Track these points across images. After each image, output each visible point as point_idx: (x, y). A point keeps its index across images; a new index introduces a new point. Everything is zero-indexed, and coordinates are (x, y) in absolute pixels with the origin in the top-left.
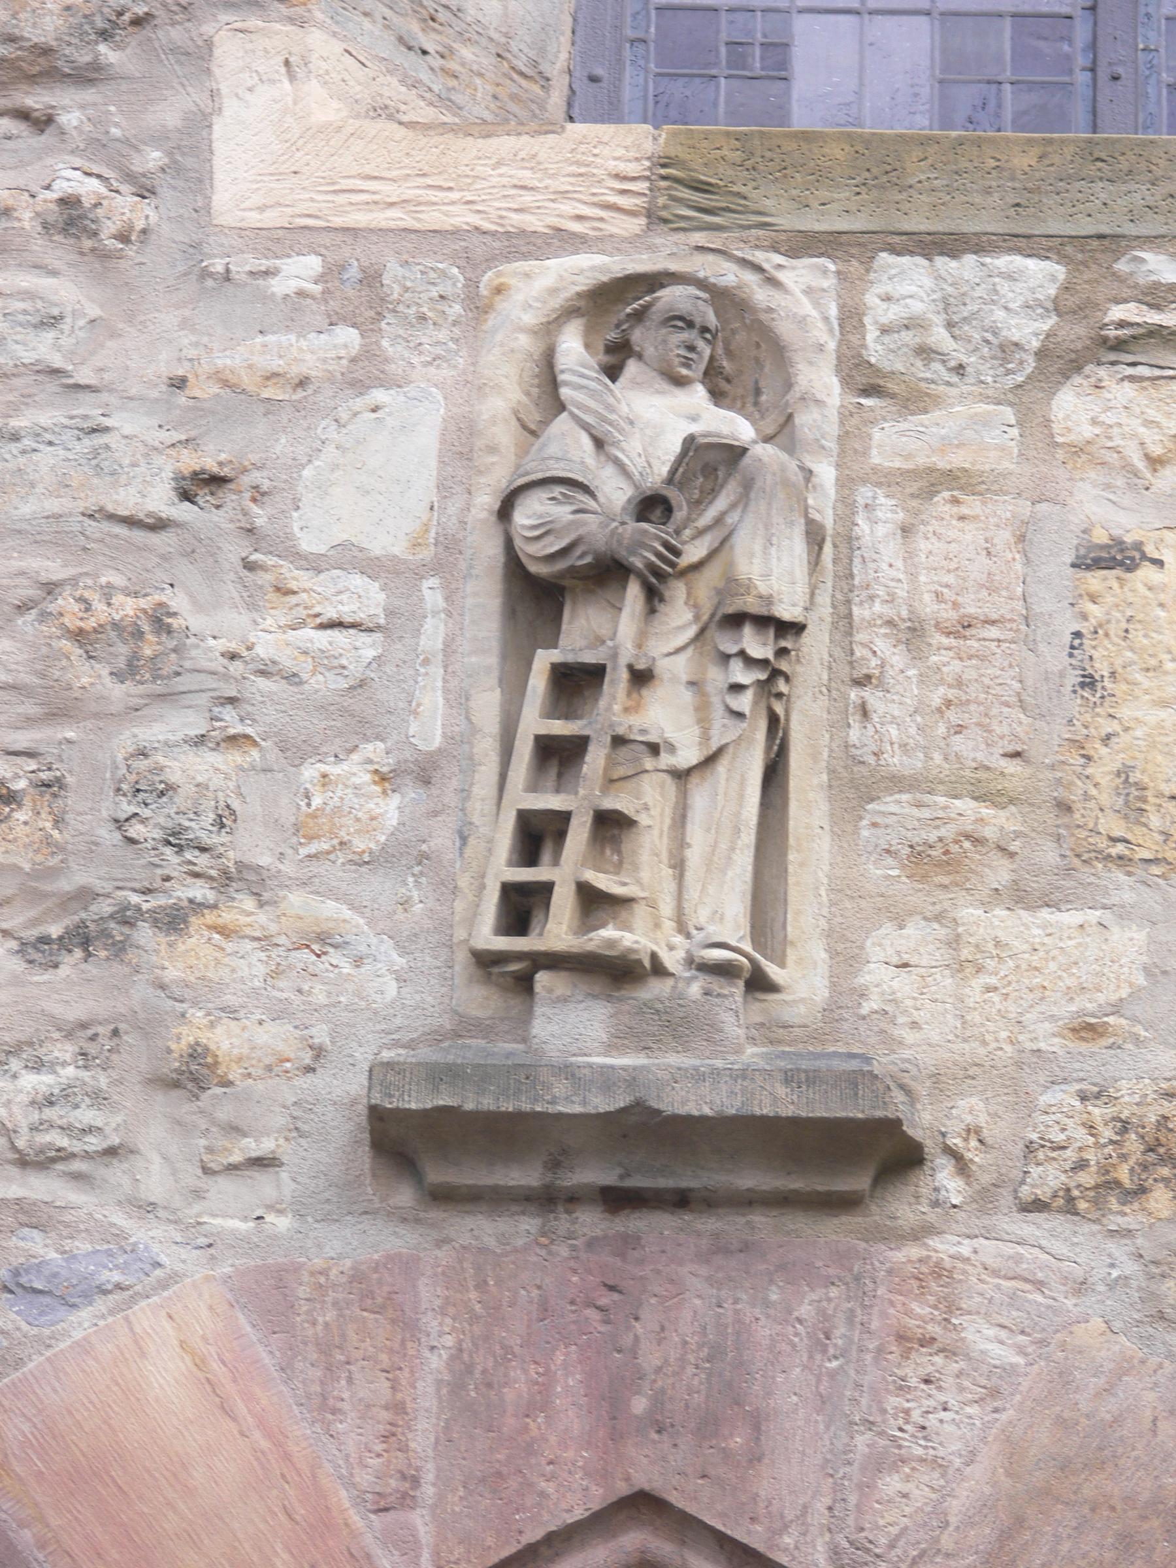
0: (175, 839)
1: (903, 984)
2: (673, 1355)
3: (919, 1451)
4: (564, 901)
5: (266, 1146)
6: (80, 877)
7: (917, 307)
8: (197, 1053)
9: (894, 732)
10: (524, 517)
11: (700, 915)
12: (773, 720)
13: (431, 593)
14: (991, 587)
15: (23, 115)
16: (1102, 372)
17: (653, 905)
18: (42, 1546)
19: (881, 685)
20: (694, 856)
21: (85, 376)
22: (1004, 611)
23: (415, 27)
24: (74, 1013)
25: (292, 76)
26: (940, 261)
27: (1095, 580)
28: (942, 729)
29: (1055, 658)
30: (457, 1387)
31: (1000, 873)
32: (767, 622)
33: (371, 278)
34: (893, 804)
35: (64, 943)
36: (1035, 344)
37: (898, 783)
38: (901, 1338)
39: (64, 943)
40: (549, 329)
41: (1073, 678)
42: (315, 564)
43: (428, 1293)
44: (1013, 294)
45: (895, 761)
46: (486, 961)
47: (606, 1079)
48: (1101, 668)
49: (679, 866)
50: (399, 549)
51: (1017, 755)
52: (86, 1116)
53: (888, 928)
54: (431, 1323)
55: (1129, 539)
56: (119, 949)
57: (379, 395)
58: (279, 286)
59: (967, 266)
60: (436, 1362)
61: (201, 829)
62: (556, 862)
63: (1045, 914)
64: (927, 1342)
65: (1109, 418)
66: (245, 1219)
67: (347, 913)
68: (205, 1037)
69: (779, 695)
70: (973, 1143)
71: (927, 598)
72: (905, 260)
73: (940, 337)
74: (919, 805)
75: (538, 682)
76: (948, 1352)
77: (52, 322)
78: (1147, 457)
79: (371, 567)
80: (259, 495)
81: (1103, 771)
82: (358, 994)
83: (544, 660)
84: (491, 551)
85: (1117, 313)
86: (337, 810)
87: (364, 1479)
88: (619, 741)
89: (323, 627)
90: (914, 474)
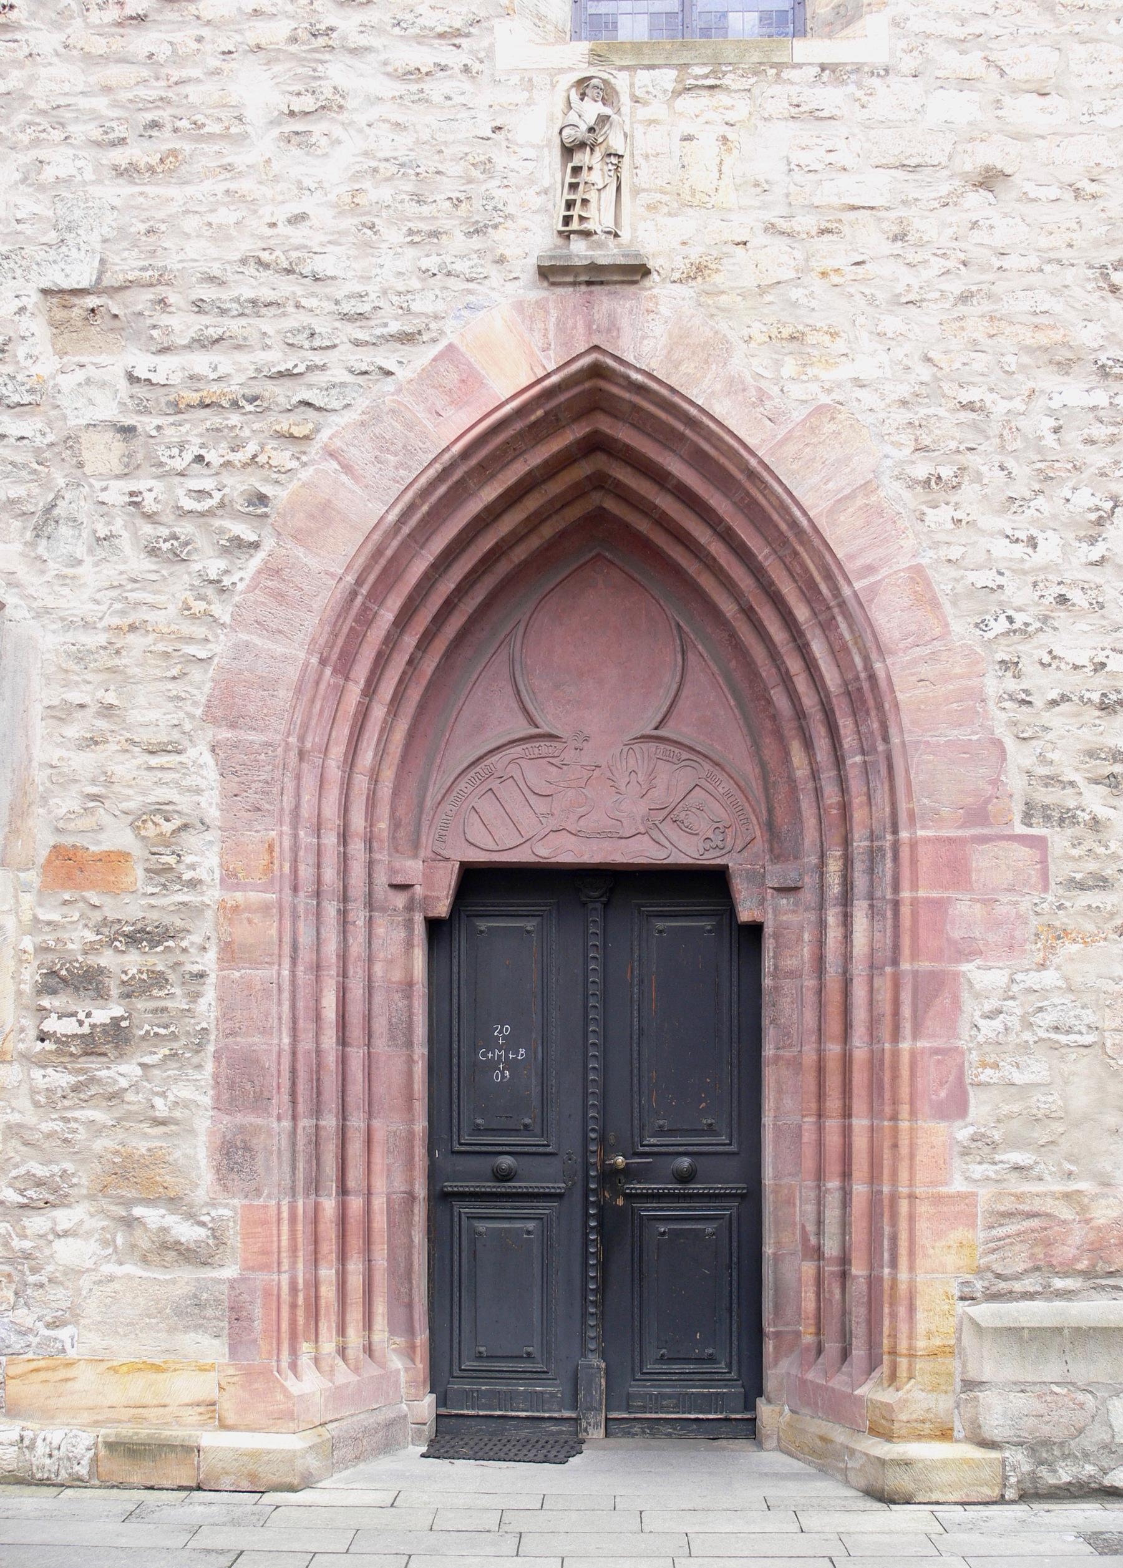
0: (495, 209)
4: (576, 219)
6: (476, 218)
8: (501, 255)
10: (565, 133)
13: (546, 150)
15: (454, 45)
21: (470, 106)
24: (476, 248)
27: (685, 143)
30: (558, 325)
31: (665, 209)
32: (615, 155)
33: (530, 80)
34: (643, 195)
37: (644, 190)
40: (569, 90)
43: (551, 305)
45: (643, 186)
46: (560, 233)
47: (586, 257)
49: (599, 210)
52: (480, 270)
54: (552, 311)
56: (485, 233)
60: (553, 319)
61: (500, 206)
73: (651, 89)
75: (569, 170)
77: (463, 93)
79: (533, 146)
80: (509, 131)
81: (687, 186)
83: (570, 165)
85: (688, 82)
87: (540, 344)
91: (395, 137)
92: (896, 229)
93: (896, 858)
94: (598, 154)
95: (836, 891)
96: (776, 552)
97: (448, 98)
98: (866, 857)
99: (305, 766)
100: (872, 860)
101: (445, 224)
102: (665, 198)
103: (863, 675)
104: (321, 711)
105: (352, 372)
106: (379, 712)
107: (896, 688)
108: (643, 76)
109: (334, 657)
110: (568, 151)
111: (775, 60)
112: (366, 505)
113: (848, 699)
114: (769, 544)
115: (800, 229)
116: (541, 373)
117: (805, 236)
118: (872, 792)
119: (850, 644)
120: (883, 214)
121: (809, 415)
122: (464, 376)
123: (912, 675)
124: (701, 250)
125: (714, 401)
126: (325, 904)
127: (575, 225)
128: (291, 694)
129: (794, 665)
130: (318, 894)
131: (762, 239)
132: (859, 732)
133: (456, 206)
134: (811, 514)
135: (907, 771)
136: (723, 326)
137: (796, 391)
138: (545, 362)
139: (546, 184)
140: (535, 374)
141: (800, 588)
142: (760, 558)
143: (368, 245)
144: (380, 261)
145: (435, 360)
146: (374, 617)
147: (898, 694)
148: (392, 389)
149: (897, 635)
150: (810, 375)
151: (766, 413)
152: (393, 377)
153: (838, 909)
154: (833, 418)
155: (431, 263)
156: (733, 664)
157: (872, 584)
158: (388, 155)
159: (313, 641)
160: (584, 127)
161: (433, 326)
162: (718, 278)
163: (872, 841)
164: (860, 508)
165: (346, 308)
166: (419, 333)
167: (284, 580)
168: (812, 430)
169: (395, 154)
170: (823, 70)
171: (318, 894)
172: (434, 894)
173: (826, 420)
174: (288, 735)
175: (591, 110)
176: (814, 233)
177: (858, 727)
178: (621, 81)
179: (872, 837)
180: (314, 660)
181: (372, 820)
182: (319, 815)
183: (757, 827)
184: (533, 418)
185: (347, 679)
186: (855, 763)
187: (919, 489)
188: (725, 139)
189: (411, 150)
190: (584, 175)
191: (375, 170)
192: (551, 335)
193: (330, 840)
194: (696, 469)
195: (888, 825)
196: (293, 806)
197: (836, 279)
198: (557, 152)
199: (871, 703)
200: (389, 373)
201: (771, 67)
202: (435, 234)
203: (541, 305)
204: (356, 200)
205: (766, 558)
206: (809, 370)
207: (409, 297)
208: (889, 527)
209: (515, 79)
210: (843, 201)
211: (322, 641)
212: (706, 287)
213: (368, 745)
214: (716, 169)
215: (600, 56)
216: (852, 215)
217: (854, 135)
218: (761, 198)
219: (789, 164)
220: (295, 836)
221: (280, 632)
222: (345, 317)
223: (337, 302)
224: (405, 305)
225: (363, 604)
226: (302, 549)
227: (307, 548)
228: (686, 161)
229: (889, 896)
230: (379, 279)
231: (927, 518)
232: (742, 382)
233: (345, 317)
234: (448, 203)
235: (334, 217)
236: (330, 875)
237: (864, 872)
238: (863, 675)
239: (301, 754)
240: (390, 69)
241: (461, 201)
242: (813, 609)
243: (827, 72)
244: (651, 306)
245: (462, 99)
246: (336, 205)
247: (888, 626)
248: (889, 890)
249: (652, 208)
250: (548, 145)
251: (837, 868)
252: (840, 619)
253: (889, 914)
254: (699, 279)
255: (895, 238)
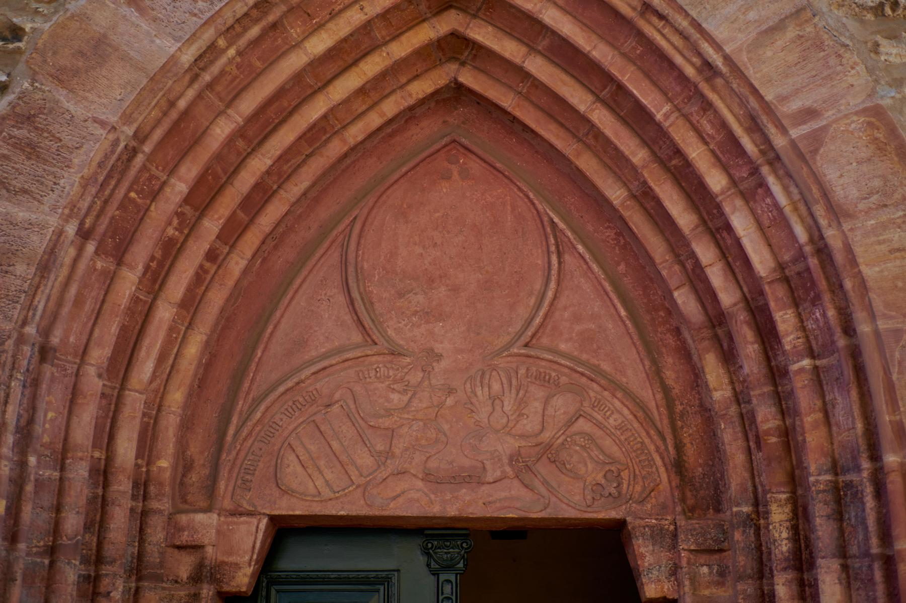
93: (880, 491)
95: (785, 549)
96: (679, 110)
98: (829, 497)
99: (48, 370)
100: (839, 501)
103: (808, 249)
104: (79, 302)
106: (165, 313)
107: (860, 260)
109: (102, 228)
112: (153, 42)
113: (786, 286)
114: (670, 100)
118: (829, 407)
119: (788, 210)
123: (880, 243)
126: (61, 564)
128: (33, 270)
129: (705, 252)
130: (52, 551)
132: (804, 329)
134: (728, 49)
135: (887, 372)
141: (712, 152)
142: (659, 117)
146: (161, 188)
147: (863, 268)
149: (854, 193)
153: (790, 575)
156: (622, 268)
157: (815, 131)
159: (73, 206)
163: (836, 474)
164: (793, 41)
167: (36, 128)
171: (52, 551)
172: (231, 559)
174: (25, 323)
177: (802, 321)
179: (835, 468)
180: (71, 229)
181: (150, 456)
182: (66, 439)
183: (662, 470)
185: (120, 262)
186: (802, 370)
187: (870, 17)
193: (79, 472)
194: (575, 17)
195: (863, 447)
196: (23, 422)
199: (823, 284)
205: (667, 116)
208: (833, 61)
211: (84, 205)
213: (148, 355)
220: (22, 464)
221: (25, 191)
225: (144, 168)
226: (65, 92)
227: (71, 91)
229: (875, 550)
231: (882, 49)
236: (72, 522)
237: (828, 517)
238: (808, 249)
239: (45, 353)
242: (730, 176)
247: (841, 181)
248: (874, 541)
251: (783, 517)
252: (771, 180)
253: (878, 575)
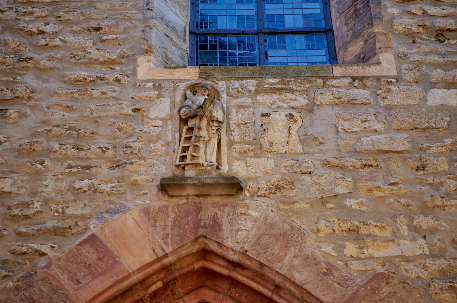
0: (132, 153)
1: (239, 168)
2: (207, 217)
3: (244, 228)
4: (189, 157)
5: (146, 191)
7: (237, 86)
9: (236, 137)
10: (182, 111)
11: (209, 159)
12: (219, 135)
13: (169, 122)
14: (249, 119)
15: (111, 68)
16: (264, 94)
17: (202, 157)
18: (111, 246)
19: (234, 131)
20: (208, 152)
21: (119, 97)
22: (251, 122)
23: (166, 60)
24: (117, 176)
25: (148, 62)
26: (240, 81)
27: (264, 118)
28: (243, 136)
29: (259, 127)
30: (175, 222)
31: (252, 154)
33: (160, 85)
34: (237, 146)
35: (116, 167)
36: (254, 90)
37: (237, 143)
38: (241, 213)
39: (116, 167)
40: (185, 91)
41: (261, 129)
42: (152, 119)
43: (170, 210)
44: (251, 84)
46: (178, 166)
48: (265, 128)
49: (205, 153)
50: (164, 117)
51: (254, 139)
52: (119, 189)
53: (236, 161)
54: (170, 214)
55: (268, 113)
57: (161, 99)
58: (147, 86)
59: (244, 82)
62: (188, 152)
63: (259, 159)
64: (244, 214)
65: (265, 99)
66: (142, 201)
67: (157, 162)
68: (136, 178)
69: (219, 132)
70: (250, 188)
71: (240, 120)
72: (235, 81)
73: (240, 90)
74: (240, 146)
76: (248, 215)
77: (115, 91)
78: (270, 103)
79: (161, 119)
82: (159, 172)
84: (177, 117)
85: (265, 86)
86: (156, 149)
87: (161, 235)
88: (196, 136)
89: (153, 127)
90: (238, 106)
91: (66, 114)
92: (418, 164)
94: (205, 121)
97: (104, 93)
101: (97, 162)
102: (251, 147)
105: (13, 253)
108: (237, 84)
110: (184, 121)
111: (322, 75)
115: (348, 164)
116: (160, 253)
117: (352, 168)
120: (406, 155)
121: (370, 281)
122: (102, 256)
124: (278, 177)
125: (294, 272)
127: (188, 161)
131: (322, 171)
133: (104, 152)
136: (298, 223)
137: (355, 266)
138: (164, 247)
139: (169, 139)
140: (156, 254)
143: (38, 172)
144: (45, 183)
145: (80, 244)
148: (43, 265)
150: (367, 254)
151: (335, 279)
152: (46, 257)
154: (388, 283)
155: (85, 184)
158: (59, 123)
160: (195, 107)
161: (80, 223)
162: (292, 194)
165: (16, 212)
166: (70, 228)
168: (373, 290)
169: (64, 123)
170: (354, 80)
173: (383, 284)
175: (200, 99)
176: (359, 167)
178: (221, 86)
184: (154, 288)
188: (291, 116)
189: (76, 121)
190: (196, 132)
191: (49, 131)
192: (169, 229)
197: (377, 193)
198: (177, 122)
200: (42, 254)
201: (319, 79)
202: (88, 167)
203: (163, 210)
204: (33, 148)
206: (365, 250)
207: (65, 205)
209: (150, 85)
210: (377, 148)
212: (283, 199)
214: (286, 132)
215: (206, 73)
216: (385, 156)
217: (379, 113)
218: (319, 147)
219: (336, 127)
222: (15, 218)
223: (9, 208)
224: (60, 210)
228: (265, 127)
230: (43, 194)
232: (315, 259)
233: (15, 218)
234: (99, 150)
235: (16, 157)
240: (66, 79)
241: (108, 149)
243: (357, 81)
244: (243, 210)
245: (113, 94)
246: (18, 150)
249: (243, 153)
250: (171, 117)
254: (278, 194)
255: (418, 169)
